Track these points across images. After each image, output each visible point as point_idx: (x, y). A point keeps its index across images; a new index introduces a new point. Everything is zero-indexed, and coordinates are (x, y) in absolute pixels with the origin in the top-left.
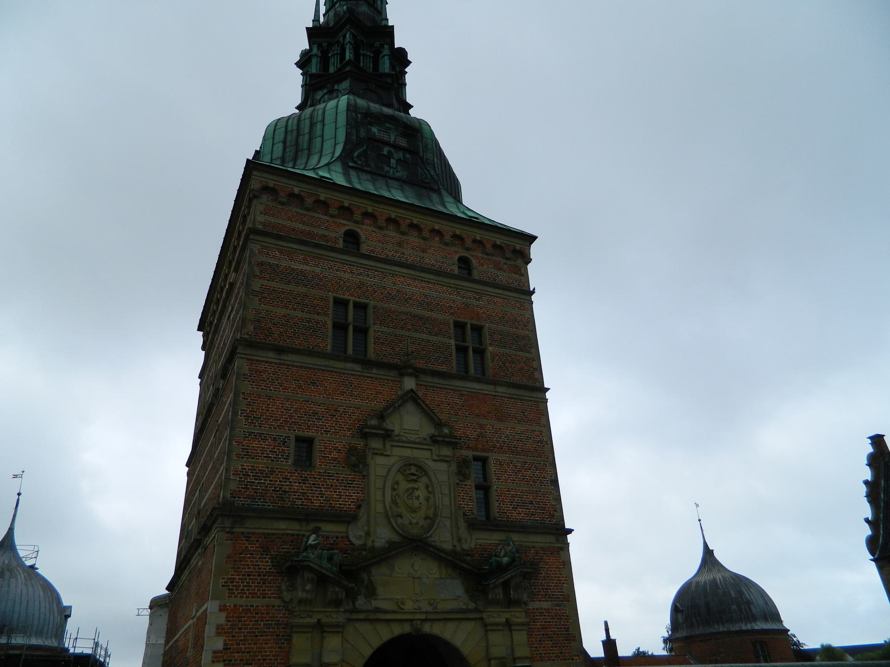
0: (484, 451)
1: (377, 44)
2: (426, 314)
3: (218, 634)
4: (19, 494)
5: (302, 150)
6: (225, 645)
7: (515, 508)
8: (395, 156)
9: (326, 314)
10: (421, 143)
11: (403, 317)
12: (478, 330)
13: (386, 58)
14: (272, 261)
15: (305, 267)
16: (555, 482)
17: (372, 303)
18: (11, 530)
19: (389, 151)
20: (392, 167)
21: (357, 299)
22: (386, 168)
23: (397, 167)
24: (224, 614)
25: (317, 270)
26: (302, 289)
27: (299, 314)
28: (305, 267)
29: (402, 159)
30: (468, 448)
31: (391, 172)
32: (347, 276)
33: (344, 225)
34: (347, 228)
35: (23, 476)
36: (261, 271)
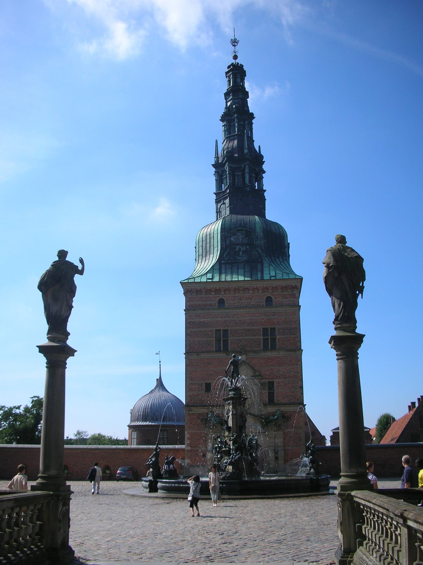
0: (272, 379)
1: (243, 166)
2: (251, 327)
3: (188, 440)
4: (160, 362)
5: (208, 252)
6: (190, 442)
7: (283, 399)
8: (242, 250)
9: (213, 337)
10: (255, 236)
11: (242, 331)
12: (273, 330)
13: (247, 174)
14: (193, 321)
15: (204, 320)
16: (302, 387)
17: (229, 328)
18: (160, 377)
19: (239, 248)
20: (241, 256)
21: (224, 328)
22: (238, 258)
23: (243, 255)
24: (189, 435)
25: (209, 320)
26: (204, 329)
27: (204, 339)
28: (204, 320)
29: (245, 250)
30: (266, 379)
31: (240, 259)
32: (220, 319)
33: (218, 297)
34: (219, 298)
35: (160, 354)
36: (190, 325)
